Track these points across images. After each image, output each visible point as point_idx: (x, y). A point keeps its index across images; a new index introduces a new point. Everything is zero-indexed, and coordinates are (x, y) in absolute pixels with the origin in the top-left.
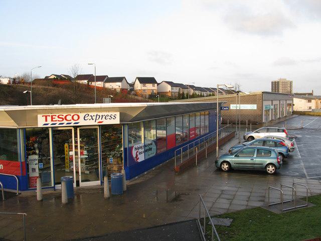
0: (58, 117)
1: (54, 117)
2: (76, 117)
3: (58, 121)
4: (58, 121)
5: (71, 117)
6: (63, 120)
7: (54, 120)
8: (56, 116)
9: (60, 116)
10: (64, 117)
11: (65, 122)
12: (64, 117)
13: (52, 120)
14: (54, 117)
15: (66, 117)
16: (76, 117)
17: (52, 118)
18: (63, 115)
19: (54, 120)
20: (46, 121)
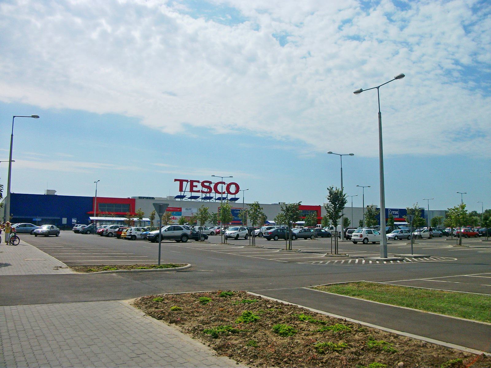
0: (203, 185)
1: (195, 184)
2: (233, 189)
3: (203, 192)
4: (203, 192)
5: (225, 187)
6: (210, 192)
7: (195, 189)
8: (198, 182)
9: (206, 184)
10: (212, 186)
11: (213, 194)
12: (212, 186)
13: (192, 191)
14: (195, 184)
15: (216, 185)
16: (233, 189)
17: (192, 186)
18: (210, 183)
19: (195, 189)
20: (181, 190)
